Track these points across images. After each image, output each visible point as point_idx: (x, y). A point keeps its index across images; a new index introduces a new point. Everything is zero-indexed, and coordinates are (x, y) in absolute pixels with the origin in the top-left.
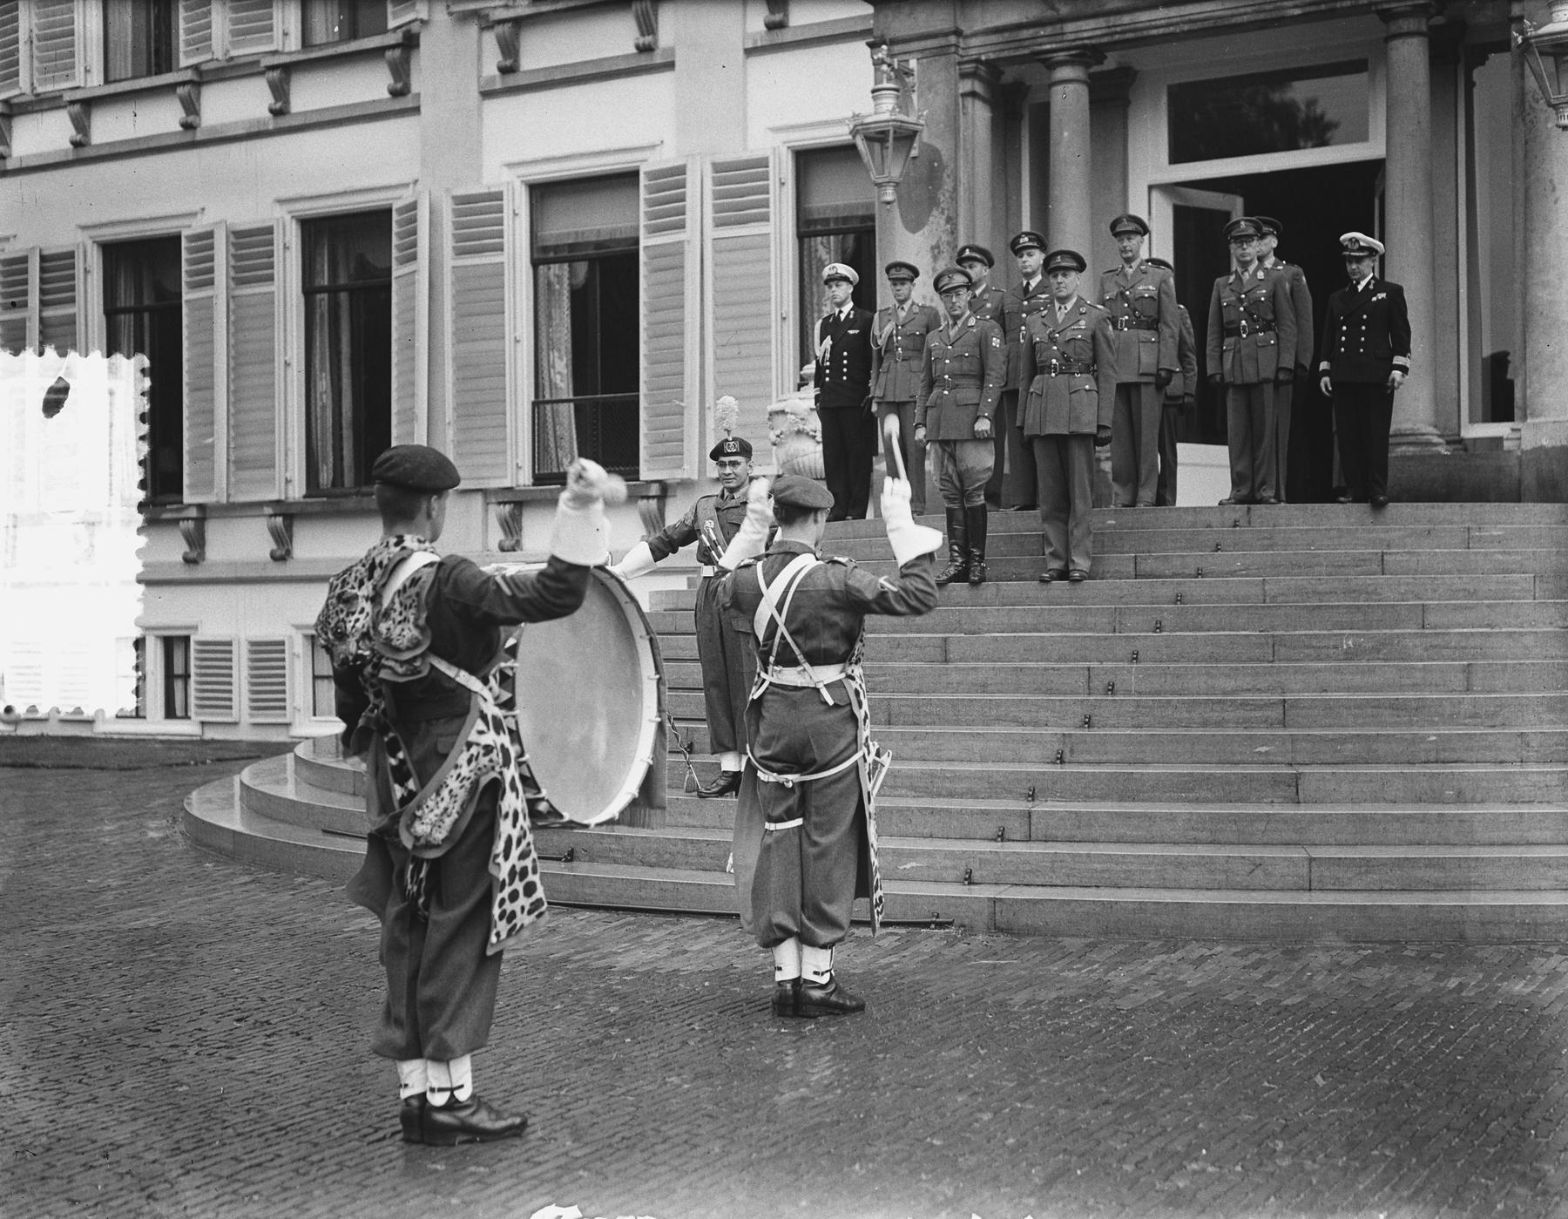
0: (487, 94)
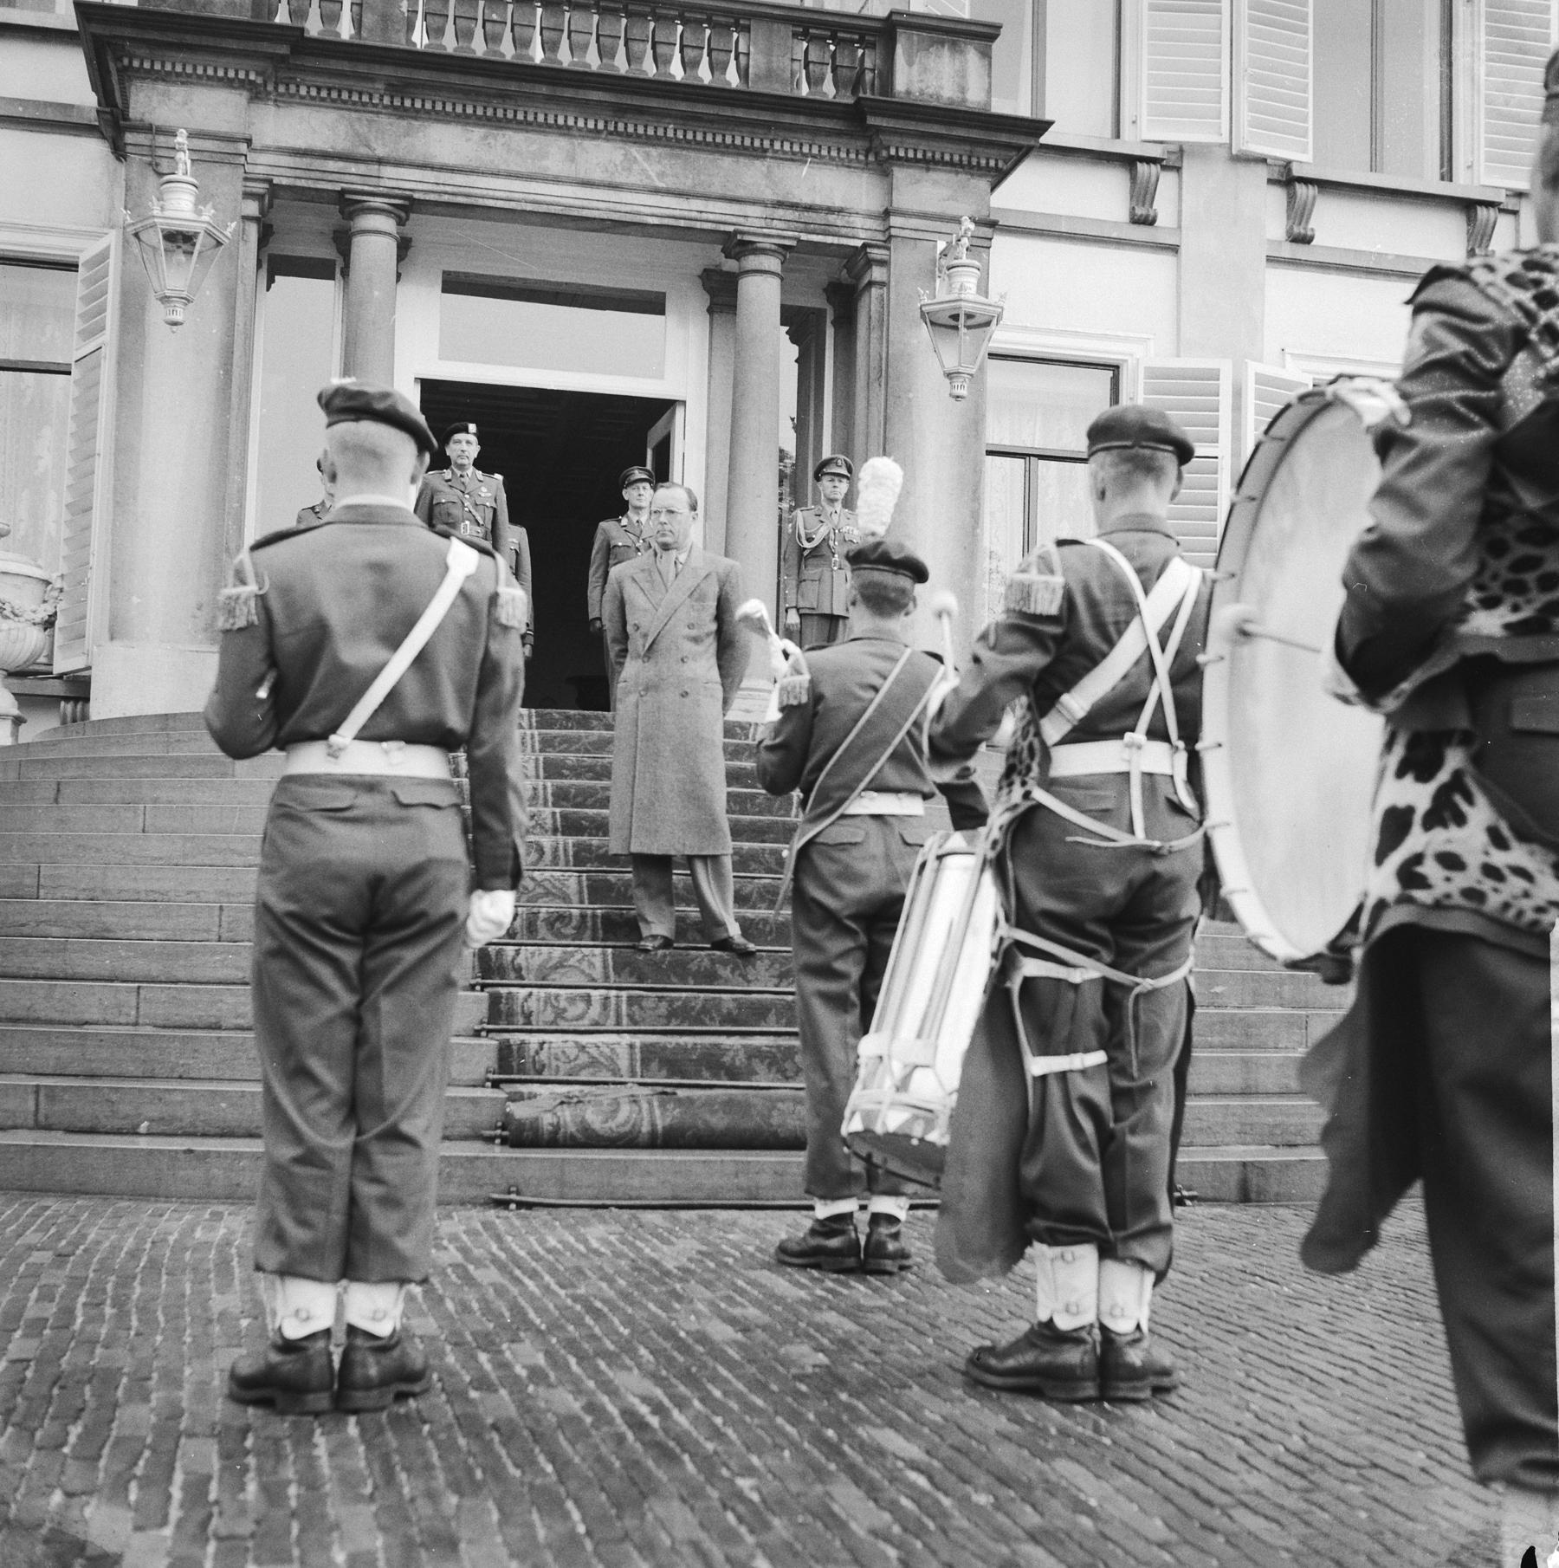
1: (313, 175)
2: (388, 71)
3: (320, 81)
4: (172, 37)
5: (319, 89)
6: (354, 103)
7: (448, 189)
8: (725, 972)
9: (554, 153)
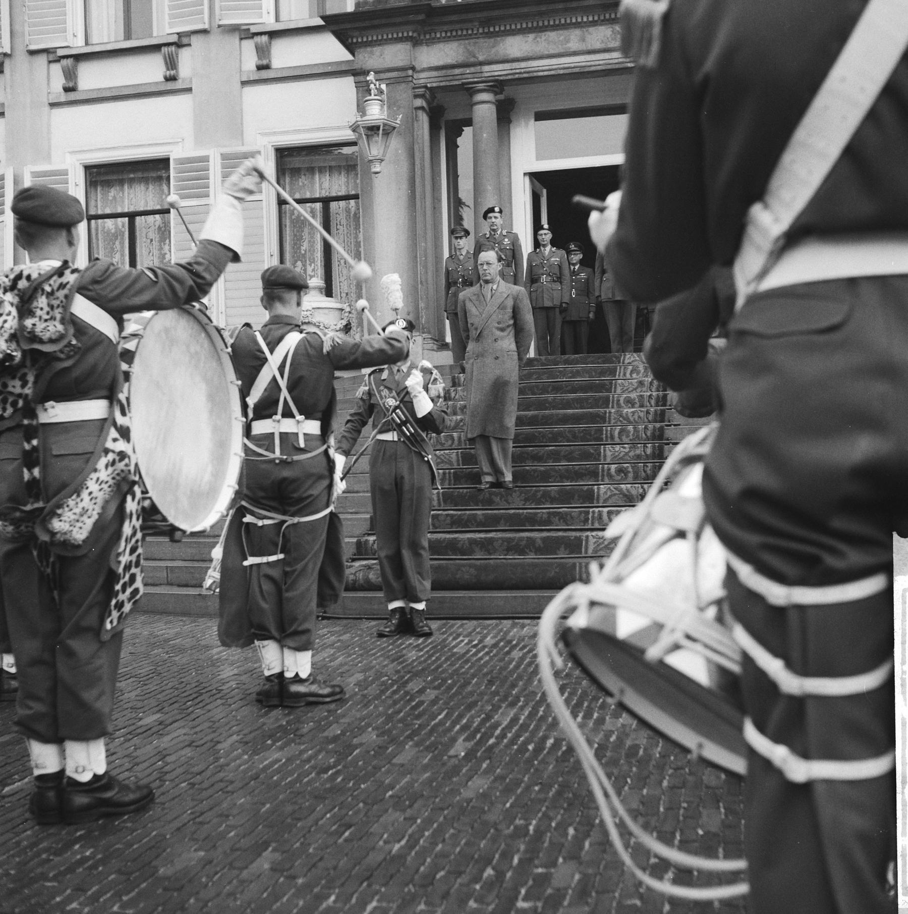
0: (53, 105)
1: (448, 78)
2: (478, 15)
3: (445, 28)
4: (367, 24)
5: (446, 32)
6: (470, 35)
7: (518, 71)
8: (497, 499)
9: (573, 39)
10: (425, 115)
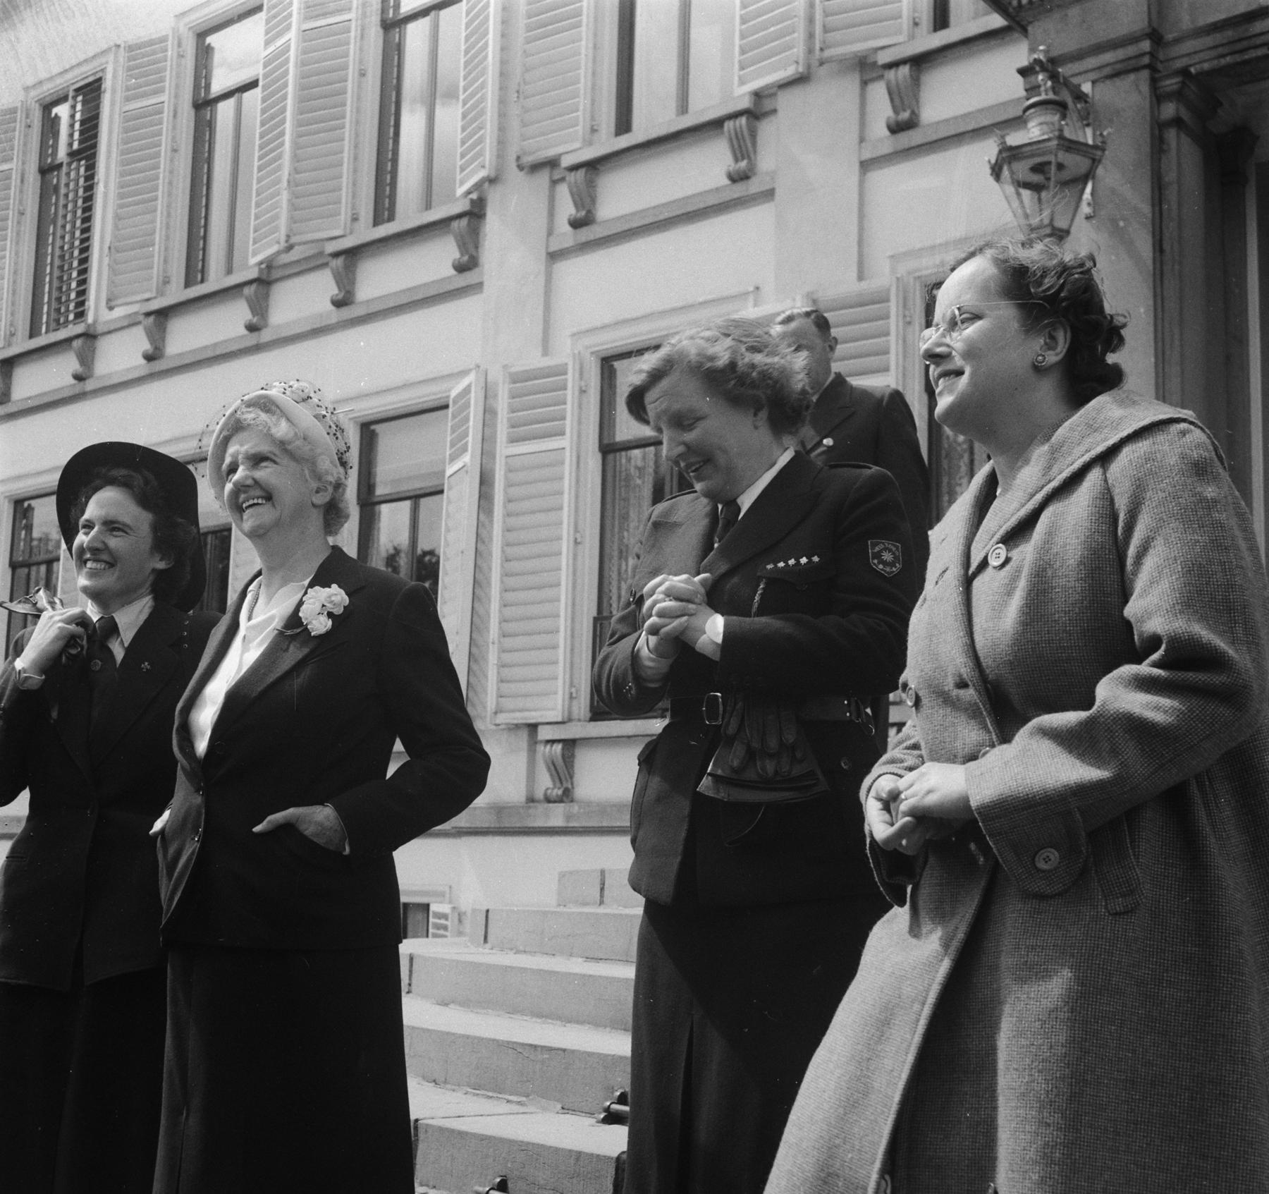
1: (1239, 46)
10: (1186, 140)
